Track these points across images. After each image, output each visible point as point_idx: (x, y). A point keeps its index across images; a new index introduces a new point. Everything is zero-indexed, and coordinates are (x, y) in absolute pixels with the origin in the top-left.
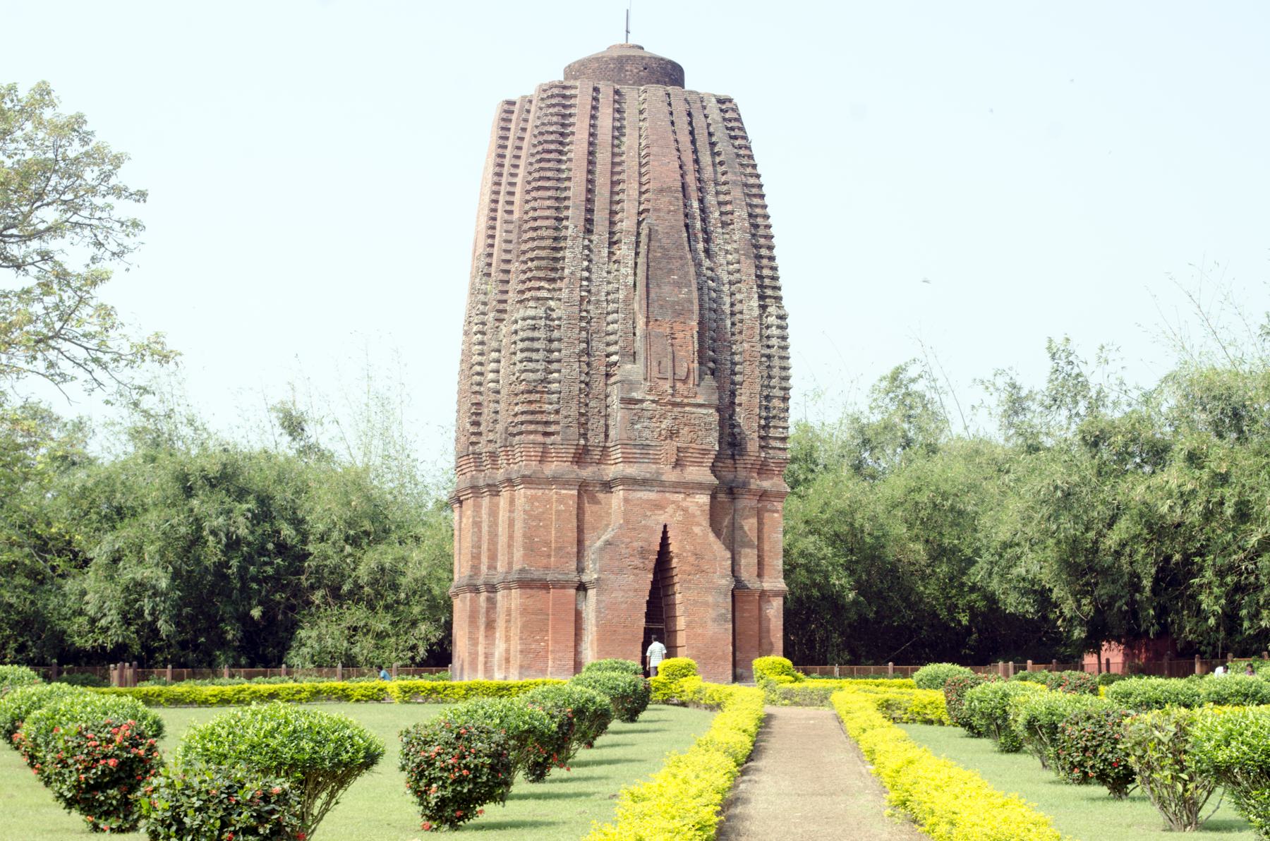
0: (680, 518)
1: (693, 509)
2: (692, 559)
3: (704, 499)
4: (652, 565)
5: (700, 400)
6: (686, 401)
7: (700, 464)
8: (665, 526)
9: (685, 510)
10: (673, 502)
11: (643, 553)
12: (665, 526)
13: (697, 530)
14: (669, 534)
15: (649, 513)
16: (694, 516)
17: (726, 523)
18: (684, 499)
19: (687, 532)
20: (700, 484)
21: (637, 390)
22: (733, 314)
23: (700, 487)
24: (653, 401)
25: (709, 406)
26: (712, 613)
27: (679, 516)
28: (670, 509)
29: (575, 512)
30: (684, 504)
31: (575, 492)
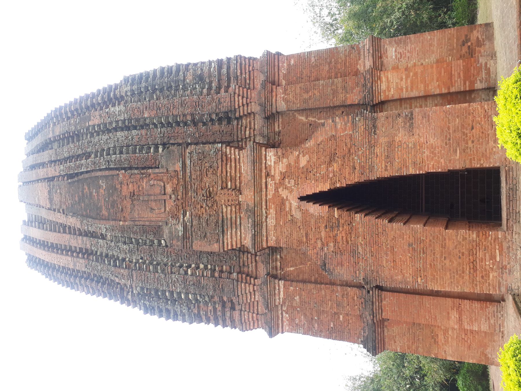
0: (292, 182)
1: (282, 167)
2: (335, 166)
3: (271, 155)
4: (345, 214)
5: (178, 166)
6: (182, 182)
7: (237, 161)
8: (302, 199)
9: (284, 176)
10: (276, 190)
11: (332, 225)
12: (302, 199)
13: (303, 161)
14: (310, 192)
15: (290, 218)
16: (289, 166)
17: (303, 118)
18: (273, 177)
19: (307, 172)
20: (254, 162)
21: (177, 230)
22: (128, 128)
23: (257, 162)
24: (184, 215)
25: (183, 157)
26: (401, 136)
27: (290, 183)
28: (284, 193)
29: (301, 285)
30: (278, 177)
31: (282, 283)
